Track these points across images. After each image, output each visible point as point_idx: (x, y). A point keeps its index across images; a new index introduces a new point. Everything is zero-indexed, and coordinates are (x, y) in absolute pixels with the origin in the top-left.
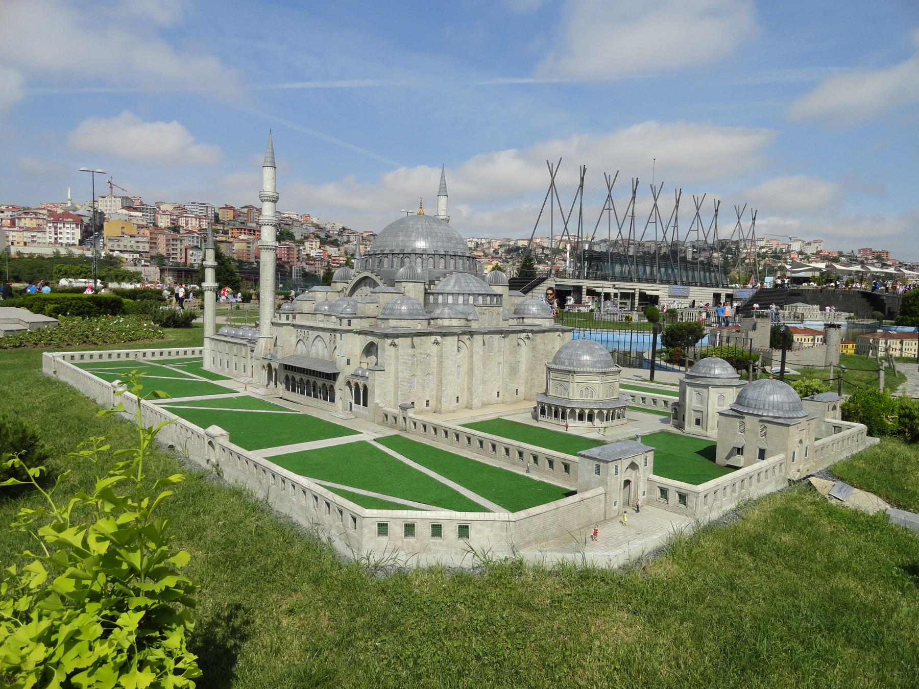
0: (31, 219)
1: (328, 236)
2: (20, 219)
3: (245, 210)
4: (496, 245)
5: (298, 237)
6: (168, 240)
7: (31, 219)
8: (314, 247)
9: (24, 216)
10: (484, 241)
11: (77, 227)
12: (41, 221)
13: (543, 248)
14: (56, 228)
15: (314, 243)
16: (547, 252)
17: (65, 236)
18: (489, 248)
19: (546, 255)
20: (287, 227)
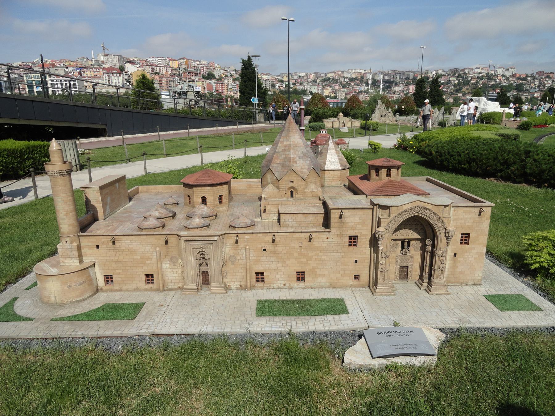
0: (91, 71)
1: (232, 76)
2: (84, 72)
3: (182, 61)
4: (312, 77)
5: (217, 77)
6: (167, 82)
7: (91, 71)
8: (230, 82)
9: (85, 70)
10: (302, 75)
11: (120, 76)
12: (96, 73)
13: (344, 78)
14: (109, 76)
15: (230, 80)
16: (347, 80)
17: (114, 81)
18: (308, 79)
19: (347, 82)
20: (209, 71)
